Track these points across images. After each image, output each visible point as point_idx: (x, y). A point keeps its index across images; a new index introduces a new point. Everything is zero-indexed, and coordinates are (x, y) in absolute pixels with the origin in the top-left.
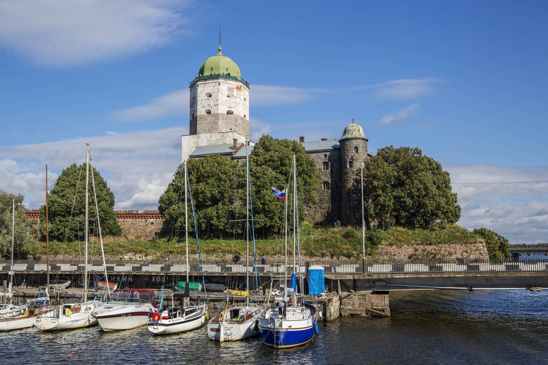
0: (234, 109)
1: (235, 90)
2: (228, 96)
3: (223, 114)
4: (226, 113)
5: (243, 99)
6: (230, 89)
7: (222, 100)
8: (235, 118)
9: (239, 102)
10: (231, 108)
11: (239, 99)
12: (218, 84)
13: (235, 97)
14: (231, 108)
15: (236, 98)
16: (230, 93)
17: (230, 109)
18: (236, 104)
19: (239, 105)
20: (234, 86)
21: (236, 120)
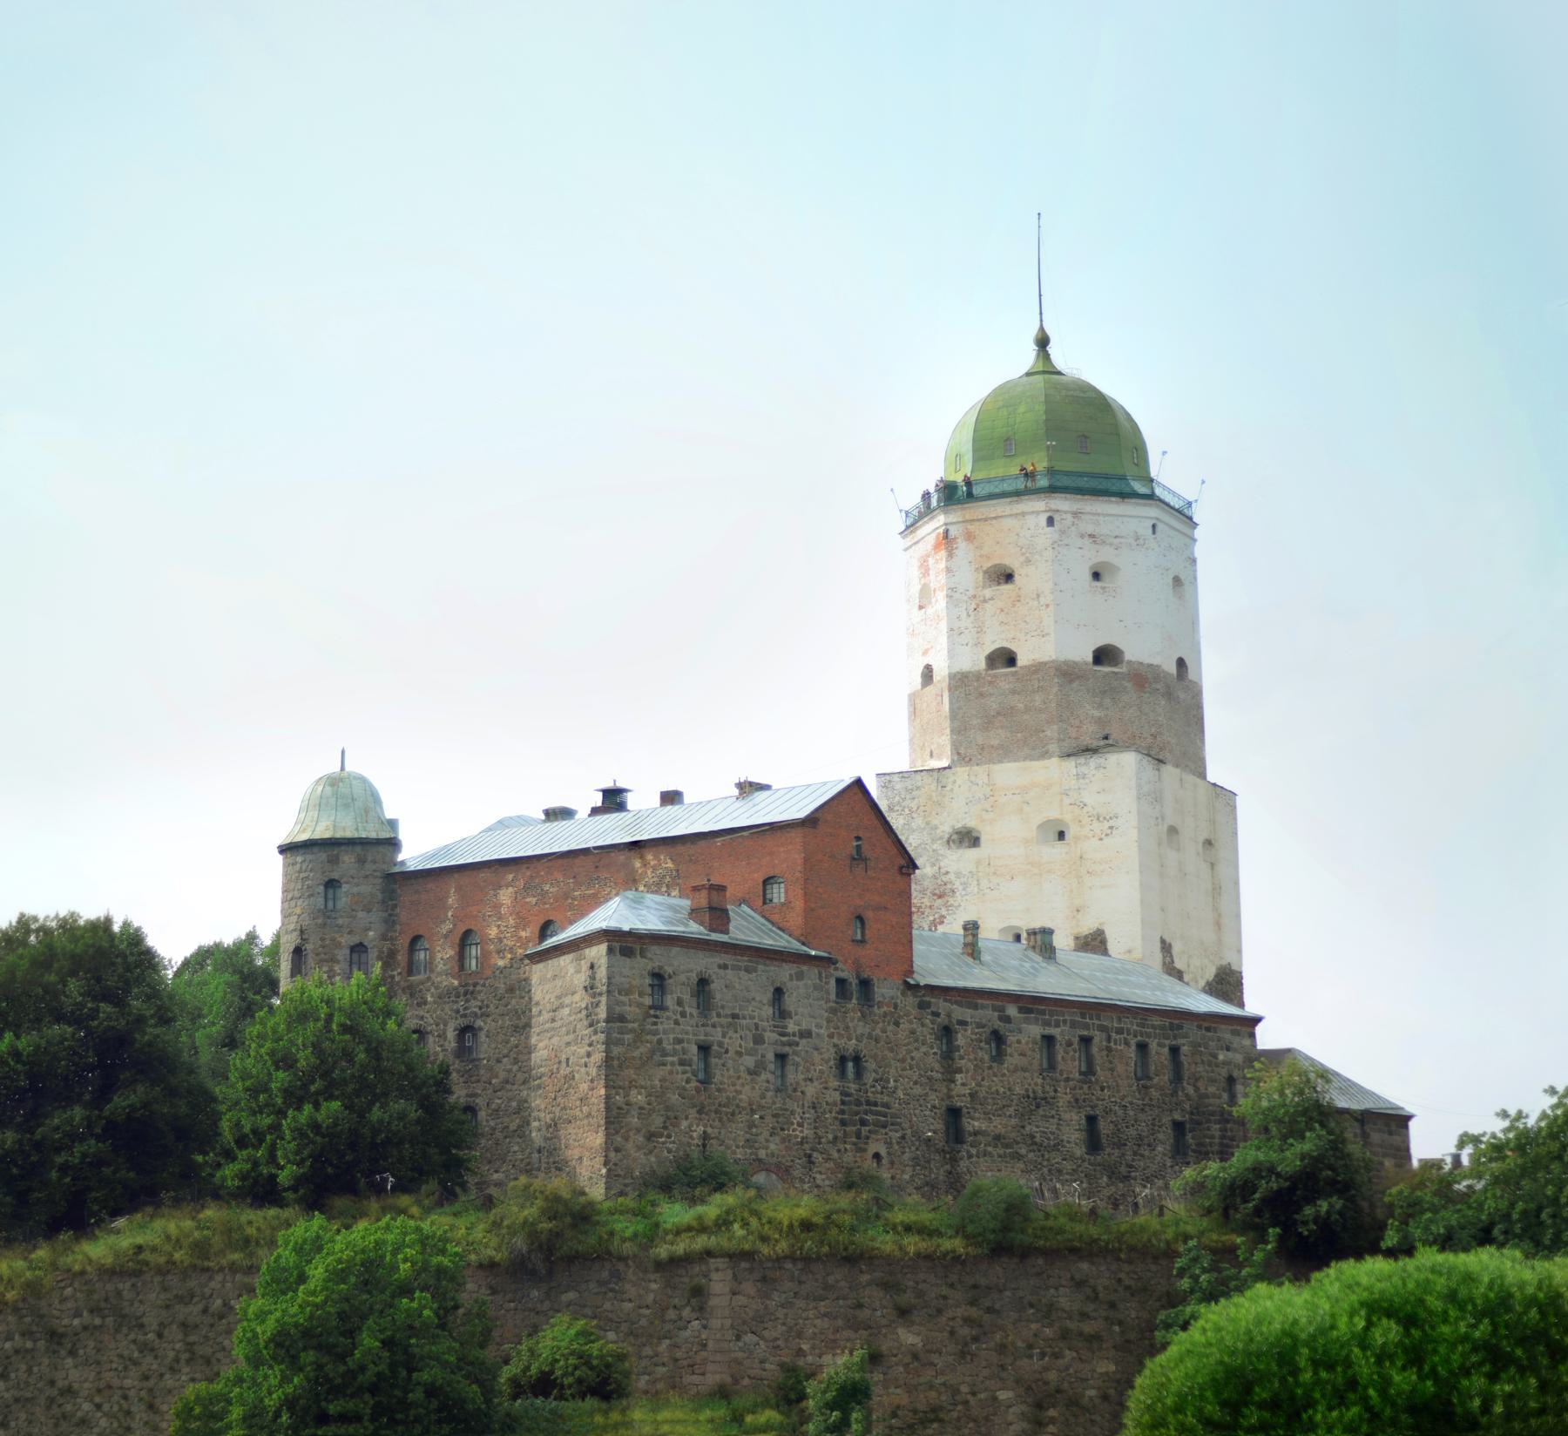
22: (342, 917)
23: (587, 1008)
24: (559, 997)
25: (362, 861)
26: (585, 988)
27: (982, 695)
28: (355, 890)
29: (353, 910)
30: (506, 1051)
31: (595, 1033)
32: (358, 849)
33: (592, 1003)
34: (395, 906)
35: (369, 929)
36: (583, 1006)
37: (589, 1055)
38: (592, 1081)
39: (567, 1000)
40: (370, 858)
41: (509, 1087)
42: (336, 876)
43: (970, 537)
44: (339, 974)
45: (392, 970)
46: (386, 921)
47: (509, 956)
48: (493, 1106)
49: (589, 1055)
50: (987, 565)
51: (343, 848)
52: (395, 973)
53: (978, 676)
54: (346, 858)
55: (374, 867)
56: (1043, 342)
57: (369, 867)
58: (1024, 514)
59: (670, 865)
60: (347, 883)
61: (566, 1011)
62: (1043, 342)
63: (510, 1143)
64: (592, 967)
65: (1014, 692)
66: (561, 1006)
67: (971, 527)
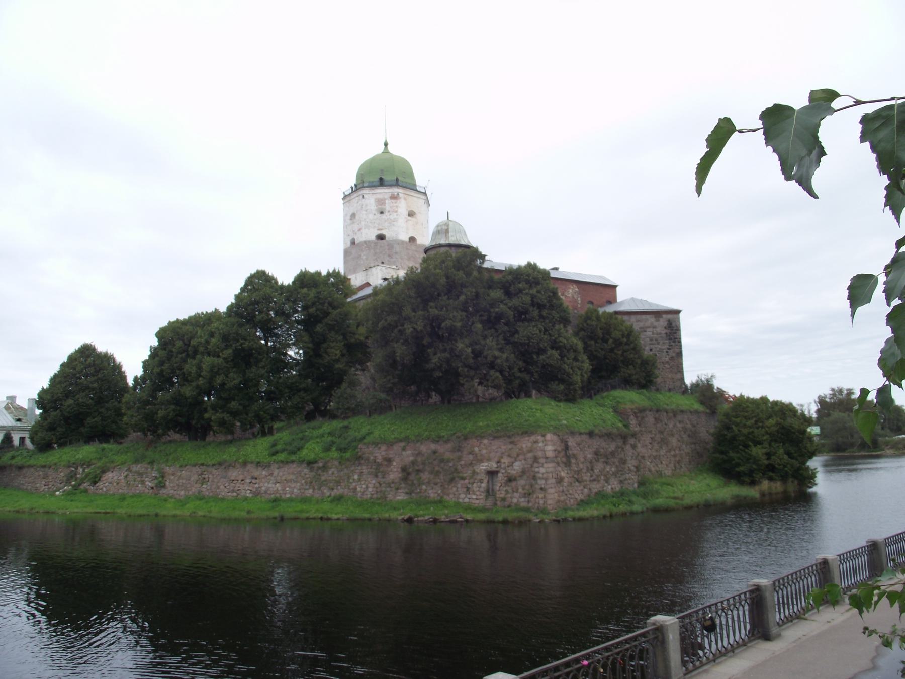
0: (387, 230)
1: (387, 201)
2: (382, 213)
3: (369, 242)
4: (373, 238)
5: (406, 213)
6: (381, 202)
7: (367, 220)
8: (388, 245)
9: (394, 219)
10: (381, 230)
11: (395, 214)
12: (361, 197)
13: (389, 211)
14: (381, 230)
15: (391, 212)
16: (380, 207)
17: (380, 232)
18: (390, 223)
19: (395, 223)
20: (387, 196)
21: (391, 246)
23: (666, 334)
24: (641, 328)
26: (665, 328)
27: (407, 249)
31: (674, 342)
33: (670, 333)
36: (663, 332)
37: (669, 349)
38: (672, 357)
39: (648, 330)
43: (405, 199)
49: (669, 349)
50: (410, 209)
53: (406, 242)
56: (386, 145)
58: (419, 198)
59: (577, 289)
61: (649, 334)
62: (386, 145)
64: (669, 321)
65: (416, 251)
66: (645, 331)
67: (406, 196)
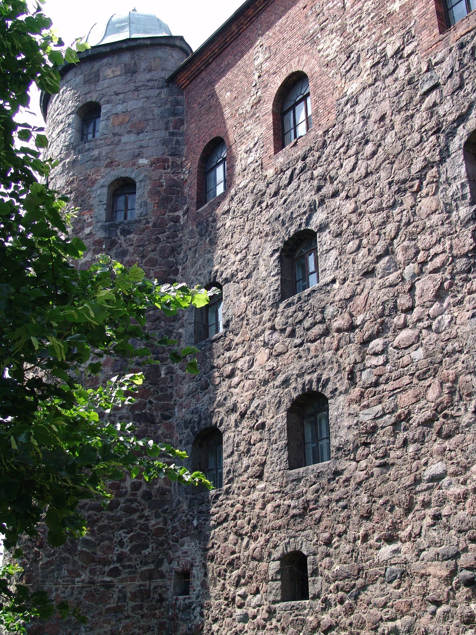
22: (97, 147)
25: (131, 71)
28: (120, 108)
29: (115, 135)
30: (380, 248)
32: (126, 58)
34: (182, 122)
35: (139, 156)
40: (143, 65)
41: (399, 320)
42: (93, 97)
44: (90, 224)
45: (175, 210)
46: (165, 143)
47: (369, 63)
48: (366, 377)
51: (105, 61)
52: (180, 213)
54: (109, 72)
55: (148, 76)
57: (142, 77)
60: (108, 102)
63: (416, 456)
